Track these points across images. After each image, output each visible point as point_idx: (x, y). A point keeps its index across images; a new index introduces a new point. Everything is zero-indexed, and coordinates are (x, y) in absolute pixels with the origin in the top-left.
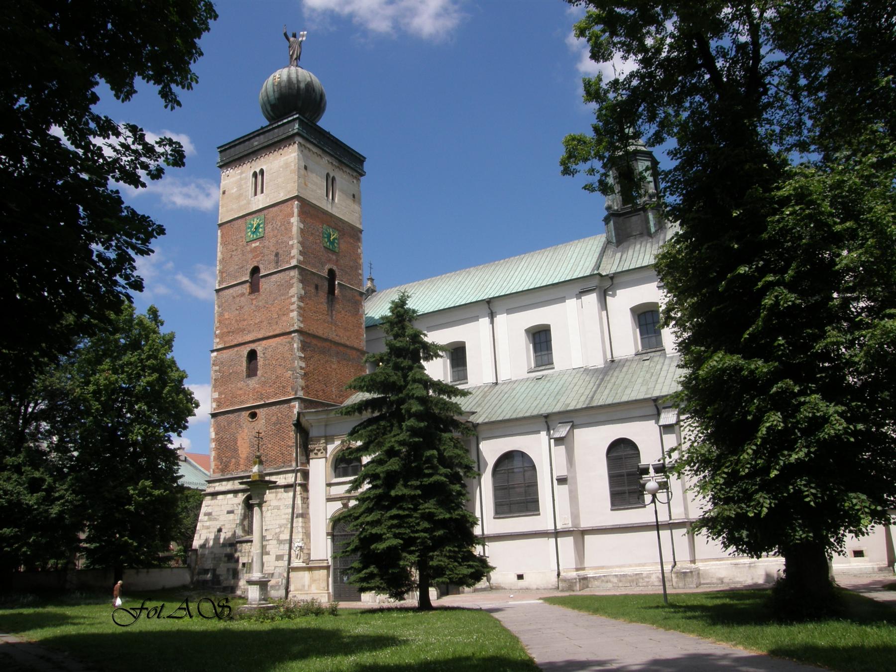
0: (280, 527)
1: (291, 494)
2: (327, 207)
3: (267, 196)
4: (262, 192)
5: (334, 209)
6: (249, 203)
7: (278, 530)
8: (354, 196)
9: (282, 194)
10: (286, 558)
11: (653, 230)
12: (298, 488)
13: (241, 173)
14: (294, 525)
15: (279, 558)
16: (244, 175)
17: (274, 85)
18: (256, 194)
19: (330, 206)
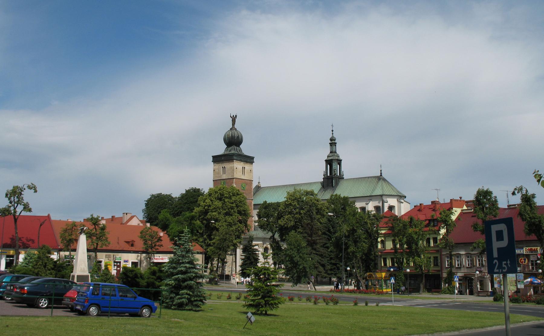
0: (230, 264)
1: (232, 256)
2: (243, 177)
3: (226, 175)
4: (225, 174)
5: (245, 177)
6: (221, 176)
7: (229, 265)
8: (251, 171)
9: (230, 176)
10: (231, 272)
11: (334, 185)
12: (234, 255)
13: (219, 166)
14: (233, 264)
15: (229, 271)
16: (220, 167)
17: (227, 137)
18: (223, 174)
19: (243, 177)
